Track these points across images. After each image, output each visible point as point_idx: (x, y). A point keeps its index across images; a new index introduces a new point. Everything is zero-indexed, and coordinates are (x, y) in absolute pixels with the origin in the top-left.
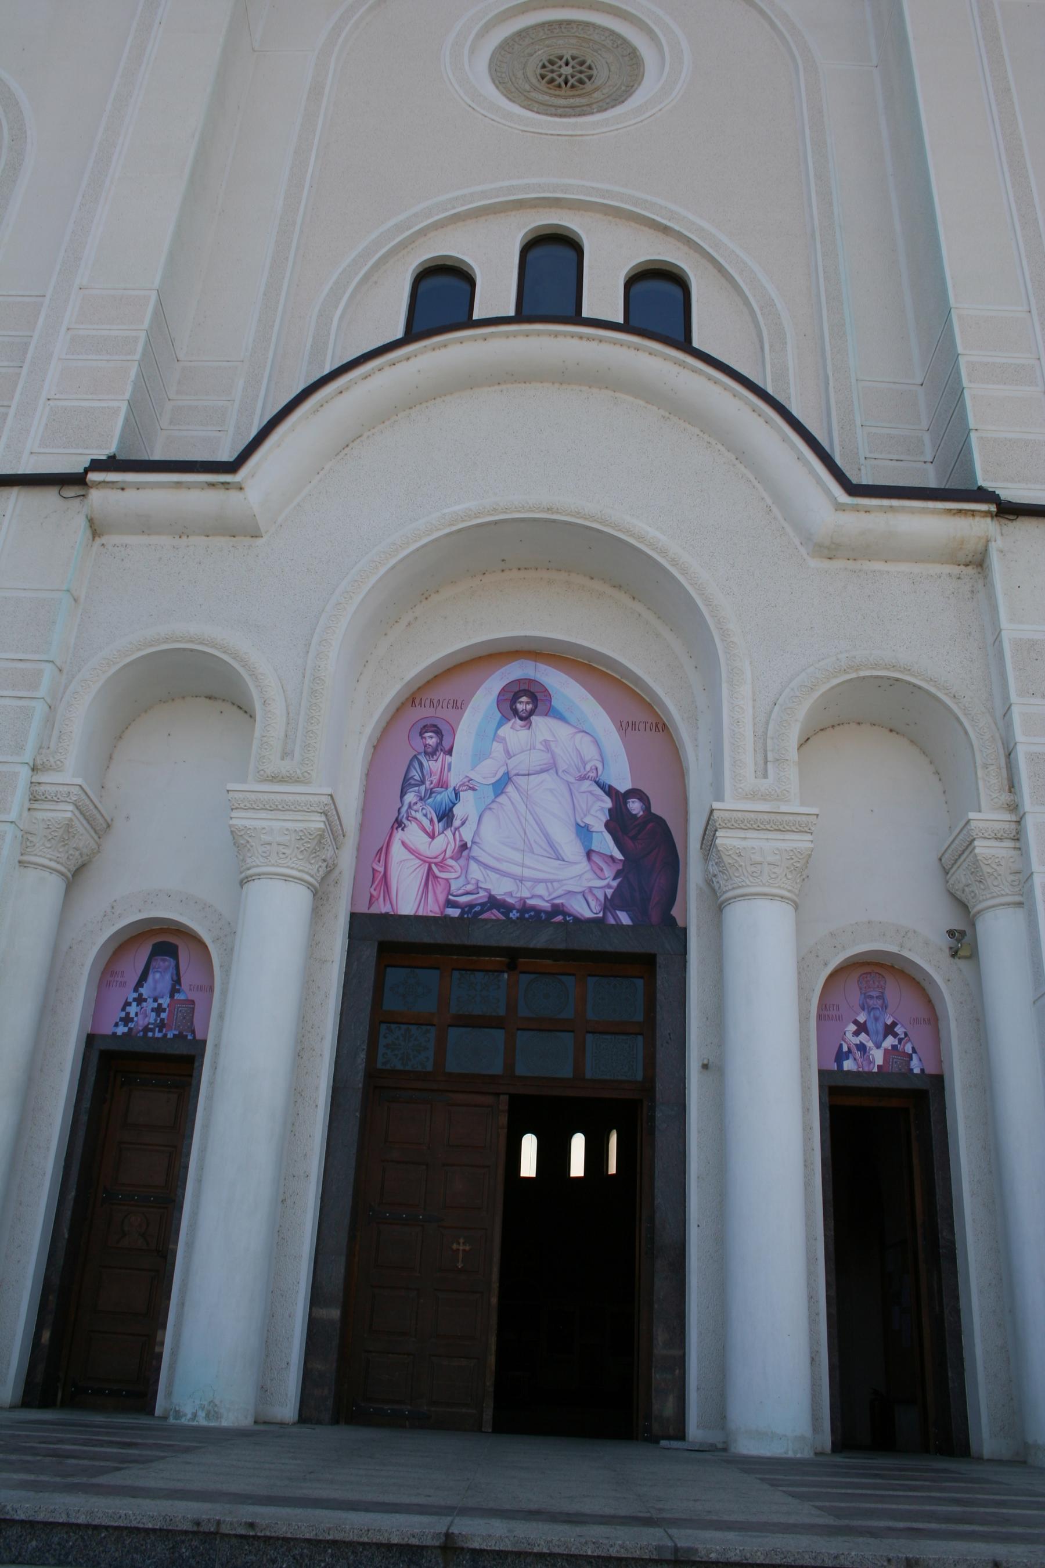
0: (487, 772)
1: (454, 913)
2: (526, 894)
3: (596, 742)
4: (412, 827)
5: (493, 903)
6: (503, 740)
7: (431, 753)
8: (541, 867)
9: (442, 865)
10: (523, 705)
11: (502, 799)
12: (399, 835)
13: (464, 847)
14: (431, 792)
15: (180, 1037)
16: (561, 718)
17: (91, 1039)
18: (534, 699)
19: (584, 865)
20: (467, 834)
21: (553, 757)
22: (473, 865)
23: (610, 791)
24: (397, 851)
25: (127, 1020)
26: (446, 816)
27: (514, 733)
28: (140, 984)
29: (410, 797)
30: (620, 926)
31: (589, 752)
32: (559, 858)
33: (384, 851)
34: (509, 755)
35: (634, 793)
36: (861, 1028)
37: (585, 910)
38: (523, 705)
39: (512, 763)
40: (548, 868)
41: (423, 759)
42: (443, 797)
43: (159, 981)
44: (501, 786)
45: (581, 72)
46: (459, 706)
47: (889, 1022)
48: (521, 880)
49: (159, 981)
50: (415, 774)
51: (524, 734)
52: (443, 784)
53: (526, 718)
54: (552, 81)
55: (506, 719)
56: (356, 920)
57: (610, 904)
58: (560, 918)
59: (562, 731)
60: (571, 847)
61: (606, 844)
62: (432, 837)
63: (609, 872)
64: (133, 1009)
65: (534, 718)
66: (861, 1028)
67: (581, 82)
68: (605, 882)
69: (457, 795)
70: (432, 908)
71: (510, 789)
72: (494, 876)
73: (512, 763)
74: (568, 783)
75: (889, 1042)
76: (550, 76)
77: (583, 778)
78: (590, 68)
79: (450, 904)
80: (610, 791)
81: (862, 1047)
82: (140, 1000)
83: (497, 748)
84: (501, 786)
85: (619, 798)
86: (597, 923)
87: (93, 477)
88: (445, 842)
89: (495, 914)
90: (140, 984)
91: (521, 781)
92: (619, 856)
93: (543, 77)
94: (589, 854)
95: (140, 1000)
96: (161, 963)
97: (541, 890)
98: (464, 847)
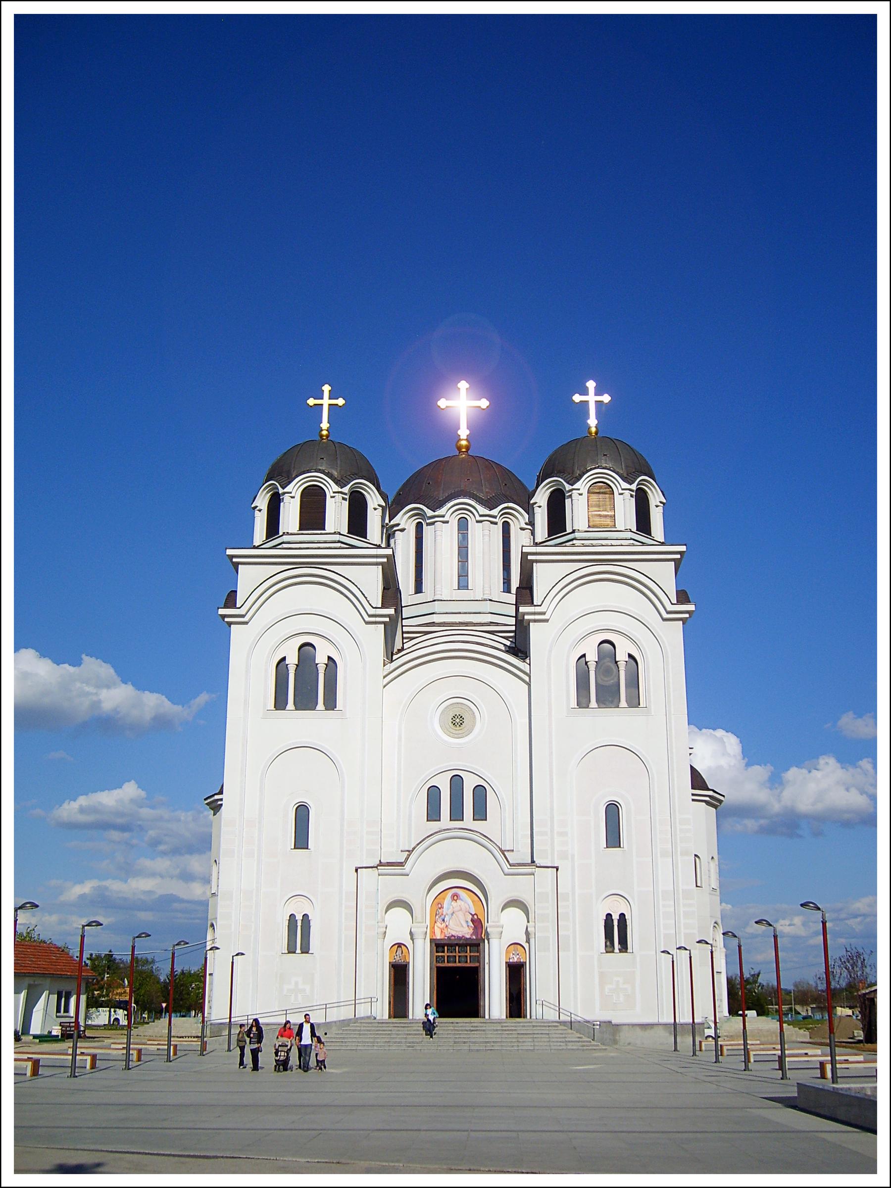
0: (450, 912)
1: (446, 938)
2: (457, 934)
3: (468, 905)
4: (438, 923)
5: (452, 936)
6: (452, 905)
7: (440, 909)
8: (458, 929)
9: (443, 929)
10: (455, 898)
11: (453, 917)
12: (436, 924)
13: (447, 926)
14: (440, 916)
15: (404, 961)
16: (462, 900)
17: (390, 963)
18: (457, 897)
19: (467, 928)
20: (447, 924)
21: (461, 908)
22: (449, 930)
23: (471, 914)
24: (436, 927)
25: (395, 959)
26: (444, 920)
27: (454, 903)
28: (396, 953)
29: (437, 917)
30: (473, 939)
31: (467, 907)
32: (462, 926)
33: (434, 927)
34: (453, 908)
35: (475, 914)
36: (513, 954)
37: (468, 936)
38: (455, 898)
39: (454, 909)
40: (461, 929)
41: (439, 910)
42: (443, 917)
43: (399, 952)
44: (452, 915)
45: (461, 720)
46: (444, 899)
47: (518, 953)
48: (456, 931)
49: (399, 952)
50: (438, 913)
51: (456, 904)
52: (442, 914)
53: (456, 901)
54: (454, 724)
55: (452, 901)
56: (431, 940)
57: (471, 935)
58: (463, 938)
59: (463, 903)
60: (465, 925)
61: (471, 924)
62: (441, 924)
63: (471, 929)
64: (395, 957)
65: (457, 901)
66: (513, 954)
67: (461, 724)
68: (471, 931)
69: (445, 916)
70: (442, 937)
71: (454, 915)
72: (452, 931)
73: (454, 909)
74: (464, 913)
75: (518, 956)
76: (454, 722)
77: (466, 912)
78: (463, 719)
79: (445, 936)
80: (471, 914)
81: (513, 958)
82: (397, 955)
83: (451, 907)
84: (452, 915)
85: (473, 915)
86: (470, 938)
87: (378, 868)
88: (444, 925)
89: (453, 938)
90: (396, 953)
91: (456, 913)
92: (473, 926)
93: (452, 722)
94: (468, 926)
95: (397, 955)
96: (399, 948)
97: (460, 933)
98: (447, 926)
